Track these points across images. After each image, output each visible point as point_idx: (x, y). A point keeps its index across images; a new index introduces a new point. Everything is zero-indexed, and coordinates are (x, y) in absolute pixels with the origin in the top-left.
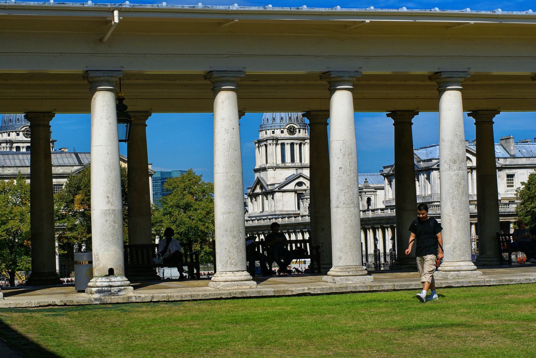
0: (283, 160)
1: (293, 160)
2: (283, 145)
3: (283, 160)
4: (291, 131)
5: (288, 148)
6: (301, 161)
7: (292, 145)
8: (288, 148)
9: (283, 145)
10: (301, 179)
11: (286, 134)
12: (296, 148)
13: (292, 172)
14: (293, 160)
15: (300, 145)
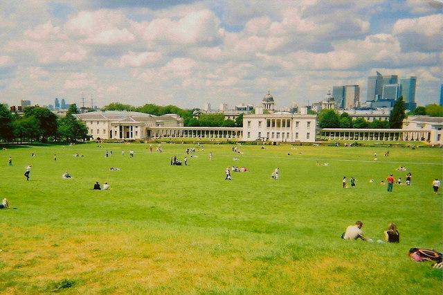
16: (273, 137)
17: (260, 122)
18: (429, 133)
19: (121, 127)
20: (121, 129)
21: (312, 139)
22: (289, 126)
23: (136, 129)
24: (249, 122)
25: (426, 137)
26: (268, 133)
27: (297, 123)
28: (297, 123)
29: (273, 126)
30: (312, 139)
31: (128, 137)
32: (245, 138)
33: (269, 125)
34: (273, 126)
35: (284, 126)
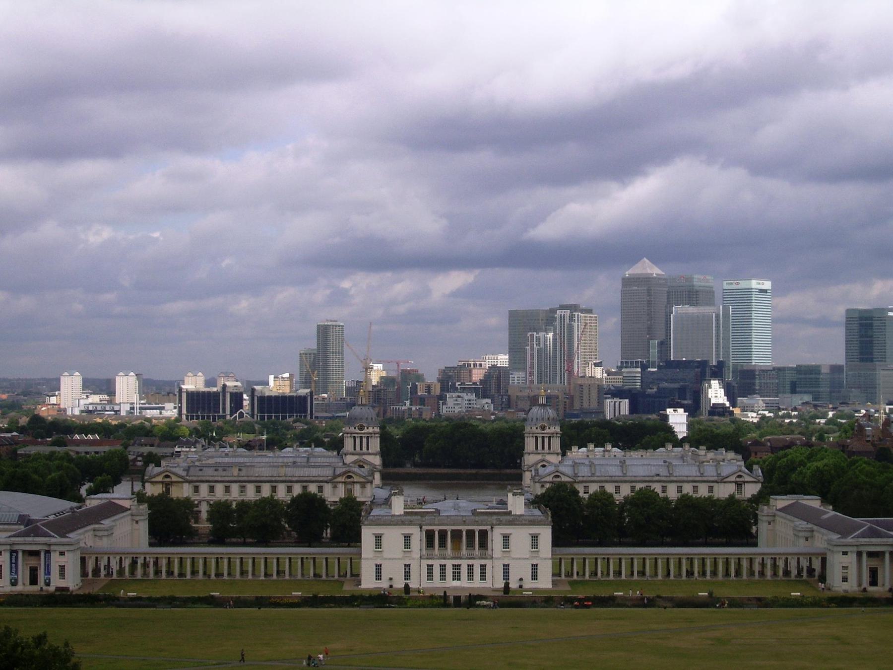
0: (537, 448)
1: (543, 448)
2: (537, 438)
3: (537, 448)
4: (543, 428)
5: (540, 440)
6: (549, 448)
7: (543, 438)
8: (540, 440)
9: (537, 438)
10: (544, 463)
11: (539, 430)
12: (546, 440)
13: (539, 457)
14: (543, 448)
15: (550, 438)
16: (443, 576)
17: (407, 538)
18: (824, 561)
19: (13, 552)
20: (14, 564)
21: (545, 582)
22: (484, 545)
23: (62, 560)
24: (378, 538)
25: (817, 565)
26: (430, 567)
27: (506, 538)
28: (506, 538)
29: (443, 544)
30: (545, 582)
31: (34, 581)
32: (368, 582)
33: (430, 543)
34: (443, 544)
35: (470, 545)
